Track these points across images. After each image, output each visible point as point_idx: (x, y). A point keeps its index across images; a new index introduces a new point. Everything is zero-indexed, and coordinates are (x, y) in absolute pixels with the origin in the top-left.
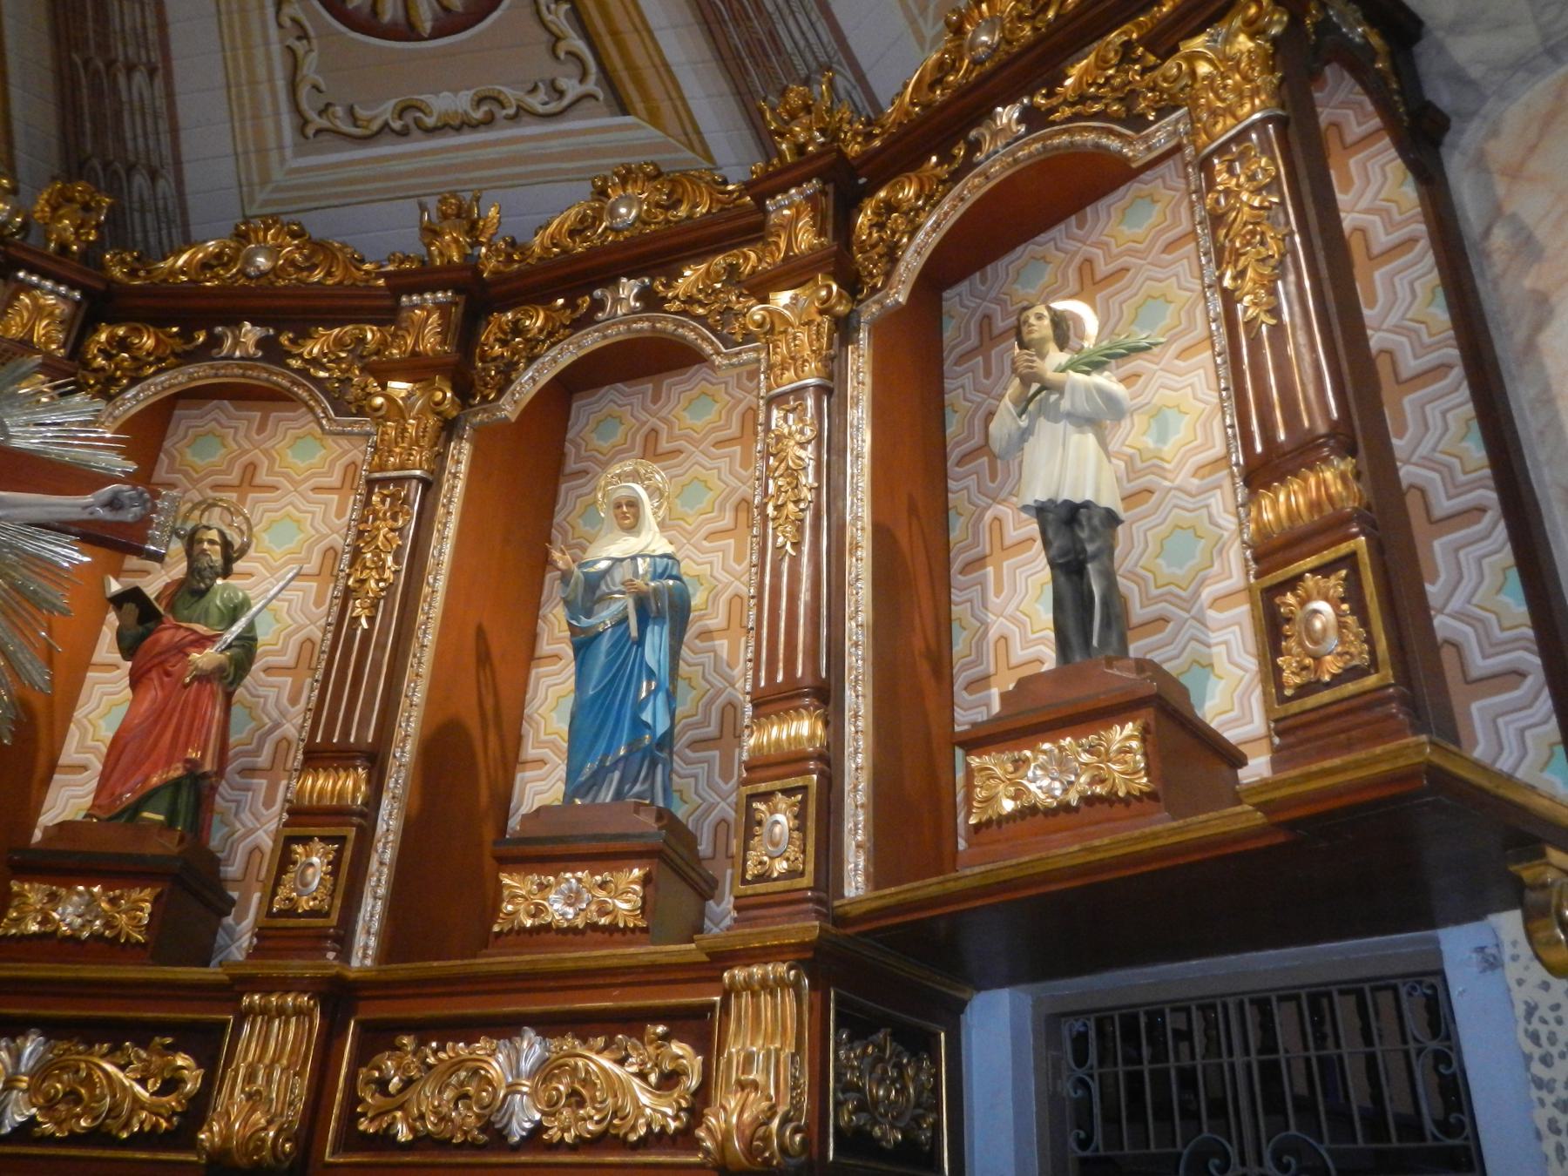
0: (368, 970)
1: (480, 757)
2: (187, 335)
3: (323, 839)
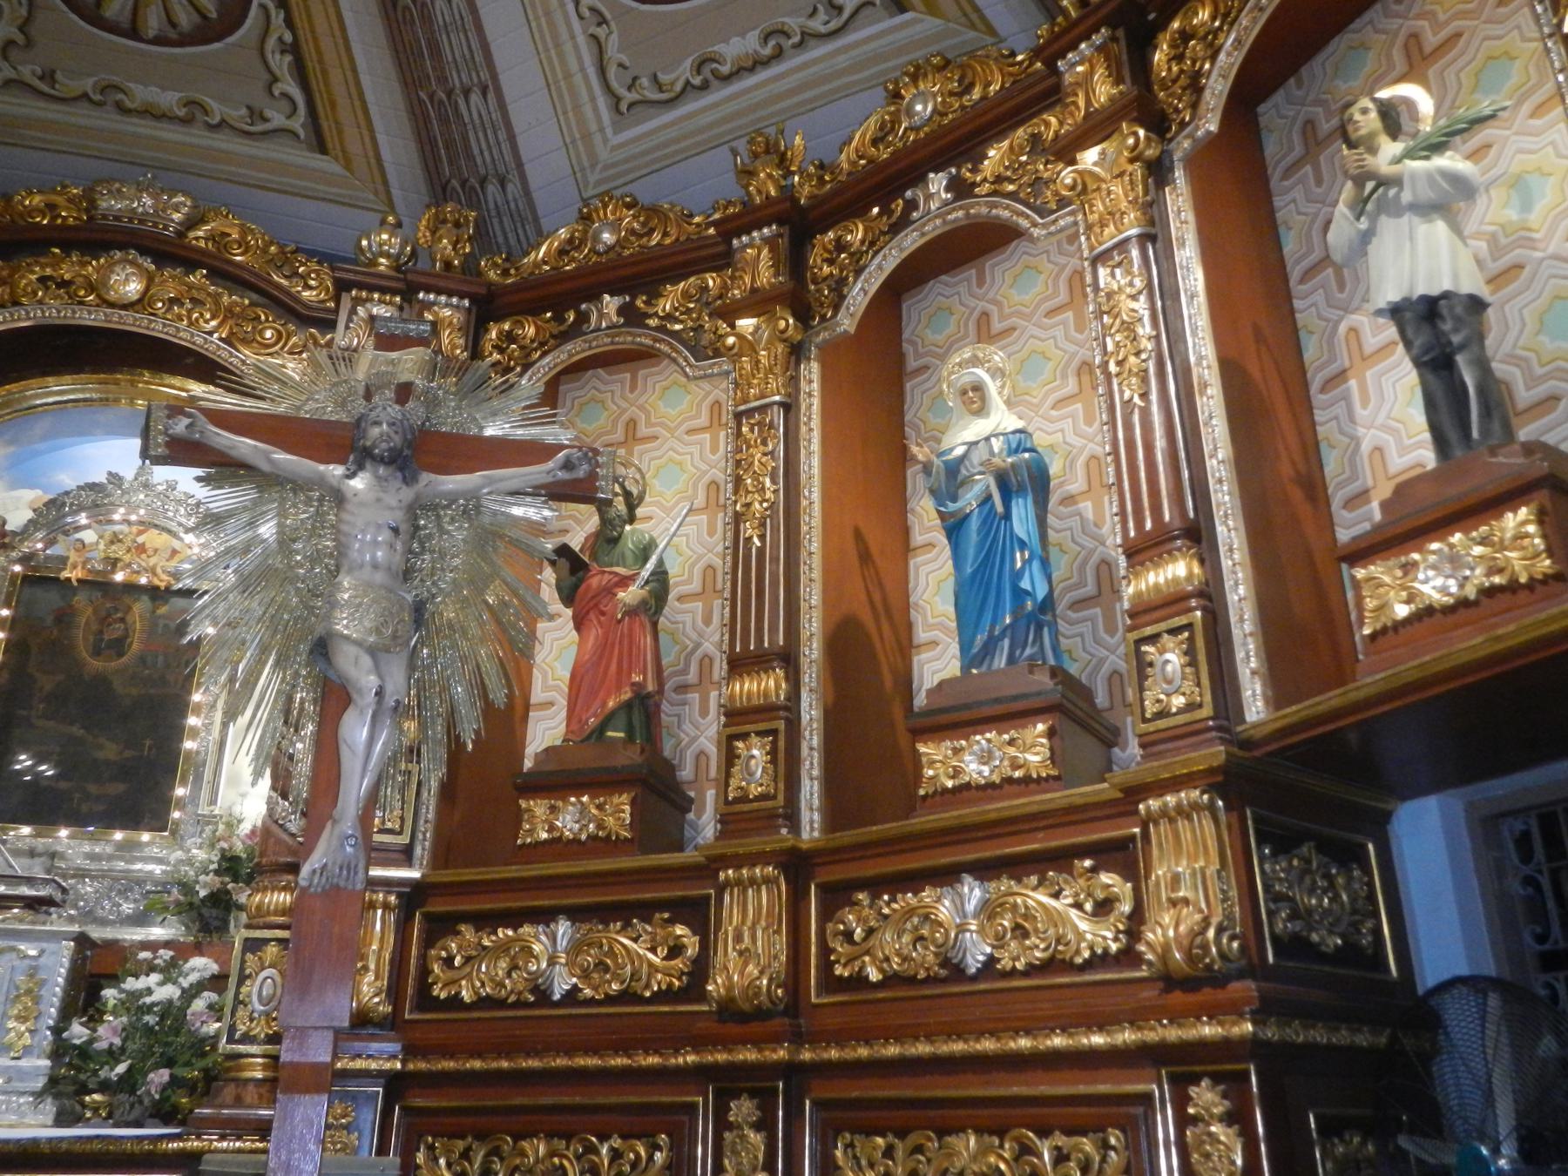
0: (818, 840)
1: (878, 645)
2: (559, 318)
3: (758, 734)
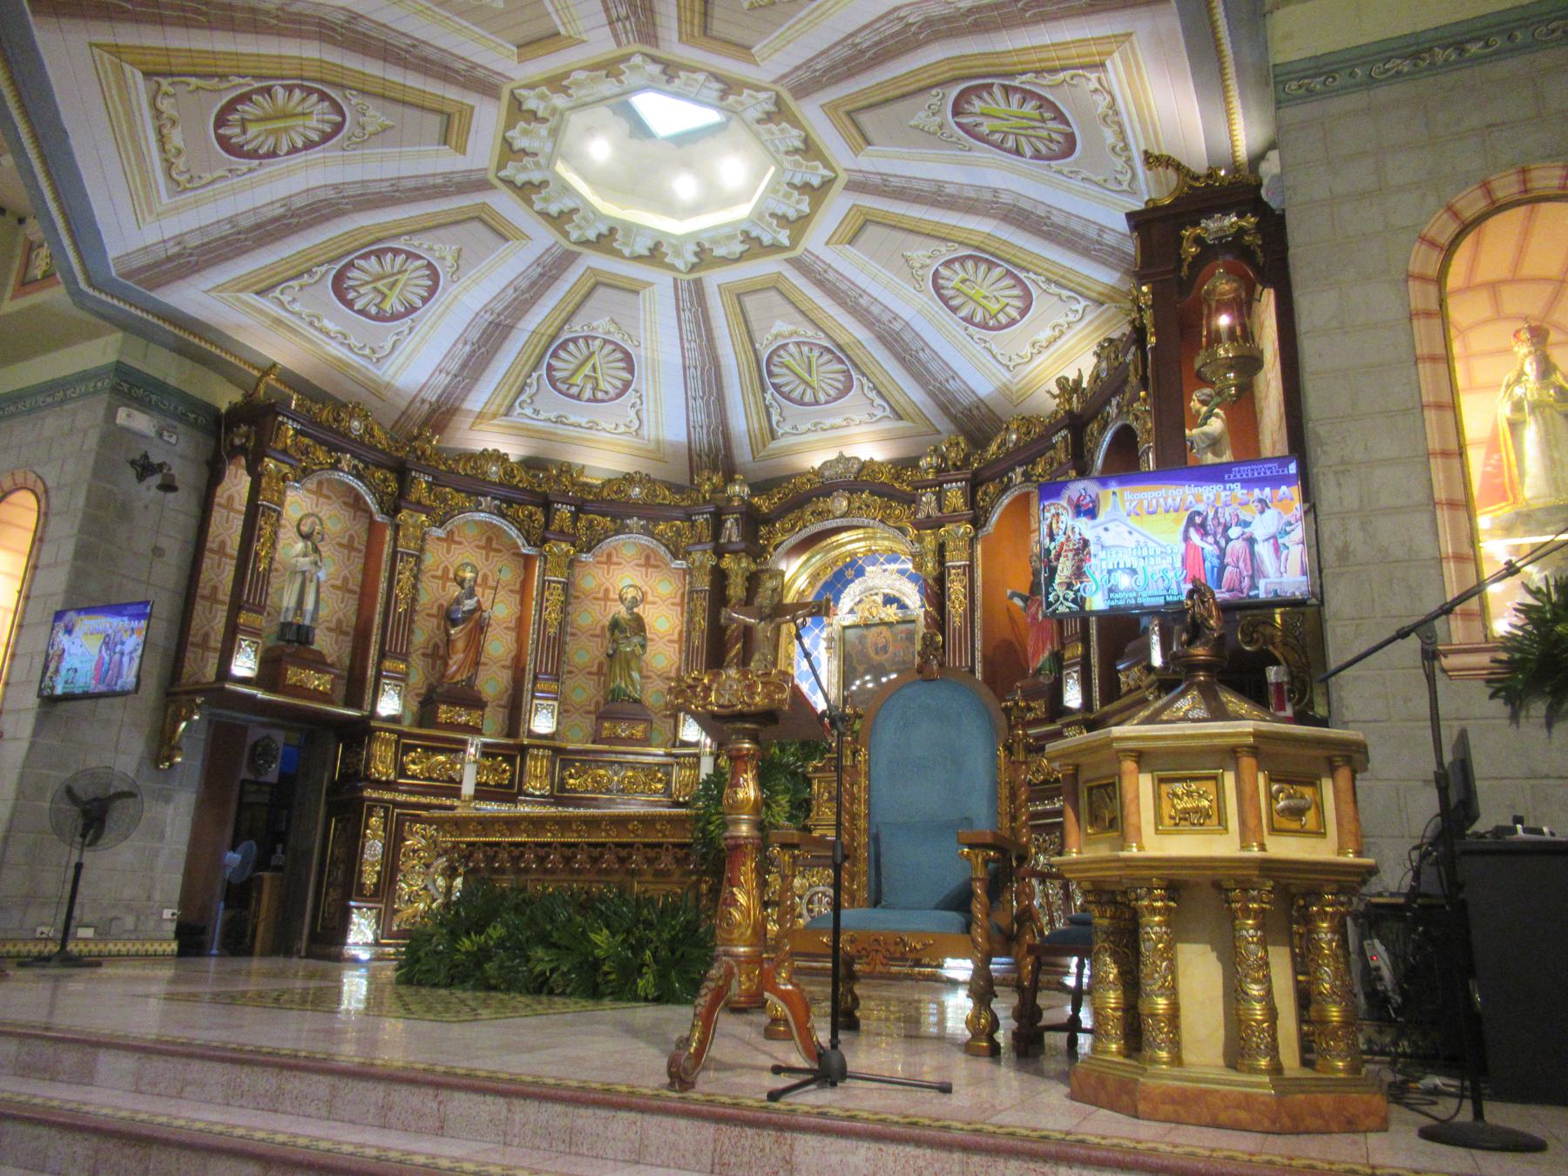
2: (1002, 482)
